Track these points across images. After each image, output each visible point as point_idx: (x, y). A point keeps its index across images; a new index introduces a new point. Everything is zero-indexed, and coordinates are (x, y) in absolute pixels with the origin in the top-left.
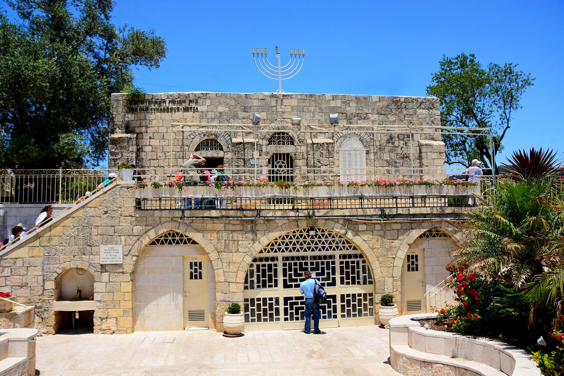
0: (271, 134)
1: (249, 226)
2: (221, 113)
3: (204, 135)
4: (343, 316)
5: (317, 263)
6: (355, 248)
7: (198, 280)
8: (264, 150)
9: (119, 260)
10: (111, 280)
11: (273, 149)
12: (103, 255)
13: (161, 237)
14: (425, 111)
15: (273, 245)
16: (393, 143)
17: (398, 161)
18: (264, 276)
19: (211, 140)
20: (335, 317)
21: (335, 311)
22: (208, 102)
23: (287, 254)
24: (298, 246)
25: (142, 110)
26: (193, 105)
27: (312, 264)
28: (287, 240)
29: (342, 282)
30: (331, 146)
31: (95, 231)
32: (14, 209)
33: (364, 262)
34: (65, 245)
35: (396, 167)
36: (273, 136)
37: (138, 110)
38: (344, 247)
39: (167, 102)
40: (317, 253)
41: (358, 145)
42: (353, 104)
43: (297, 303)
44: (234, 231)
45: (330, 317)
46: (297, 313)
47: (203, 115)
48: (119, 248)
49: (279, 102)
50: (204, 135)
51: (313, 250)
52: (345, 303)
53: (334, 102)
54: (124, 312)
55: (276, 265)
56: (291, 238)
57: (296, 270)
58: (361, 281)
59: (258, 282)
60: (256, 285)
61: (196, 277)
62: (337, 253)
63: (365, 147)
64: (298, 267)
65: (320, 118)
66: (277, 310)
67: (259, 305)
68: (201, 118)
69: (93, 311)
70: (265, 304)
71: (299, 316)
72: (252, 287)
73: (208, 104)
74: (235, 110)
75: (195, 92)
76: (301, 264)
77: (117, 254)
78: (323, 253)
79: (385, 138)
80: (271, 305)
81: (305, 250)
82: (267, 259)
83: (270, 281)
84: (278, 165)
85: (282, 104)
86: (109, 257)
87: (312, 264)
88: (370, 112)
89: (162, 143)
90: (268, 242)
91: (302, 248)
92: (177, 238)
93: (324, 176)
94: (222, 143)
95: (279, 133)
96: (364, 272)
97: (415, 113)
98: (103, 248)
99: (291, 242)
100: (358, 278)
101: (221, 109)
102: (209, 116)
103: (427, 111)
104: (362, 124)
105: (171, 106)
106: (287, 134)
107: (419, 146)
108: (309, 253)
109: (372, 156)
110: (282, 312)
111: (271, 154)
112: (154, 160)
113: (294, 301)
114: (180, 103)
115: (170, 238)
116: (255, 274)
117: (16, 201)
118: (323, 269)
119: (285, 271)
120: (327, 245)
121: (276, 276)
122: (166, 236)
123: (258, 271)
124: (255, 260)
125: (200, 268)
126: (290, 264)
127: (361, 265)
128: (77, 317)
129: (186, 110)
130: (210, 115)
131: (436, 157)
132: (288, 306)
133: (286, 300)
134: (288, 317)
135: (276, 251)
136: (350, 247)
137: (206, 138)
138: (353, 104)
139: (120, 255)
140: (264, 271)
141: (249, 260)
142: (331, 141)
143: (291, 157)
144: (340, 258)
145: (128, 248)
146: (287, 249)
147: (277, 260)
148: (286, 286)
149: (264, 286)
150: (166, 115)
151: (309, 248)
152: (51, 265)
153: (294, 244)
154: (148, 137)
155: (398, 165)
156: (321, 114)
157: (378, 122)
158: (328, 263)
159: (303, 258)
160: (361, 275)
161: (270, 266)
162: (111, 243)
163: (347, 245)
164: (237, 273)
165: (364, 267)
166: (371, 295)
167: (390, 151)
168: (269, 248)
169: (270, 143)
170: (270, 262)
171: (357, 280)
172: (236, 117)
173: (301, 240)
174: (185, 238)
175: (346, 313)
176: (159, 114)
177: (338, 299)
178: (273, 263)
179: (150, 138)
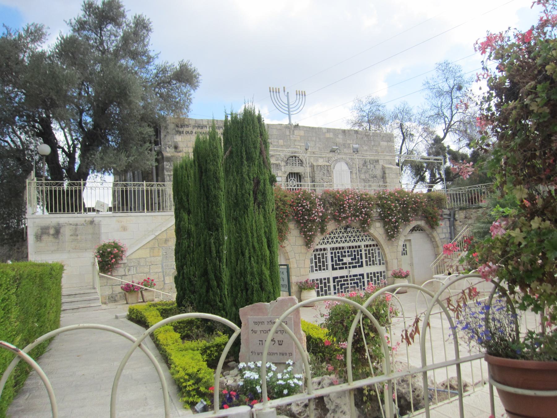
0: (287, 157)
5: (351, 251)
6: (373, 240)
11: (290, 169)
16: (367, 167)
17: (370, 179)
23: (333, 245)
25: (187, 132)
27: (348, 252)
28: (332, 236)
30: (329, 167)
33: (379, 249)
40: (351, 244)
41: (345, 167)
42: (340, 136)
46: (341, 288)
53: (328, 134)
55: (326, 254)
56: (335, 234)
58: (378, 262)
59: (316, 267)
62: (362, 244)
63: (349, 169)
66: (329, 287)
70: (321, 283)
71: (343, 290)
76: (341, 252)
78: (354, 244)
79: (362, 162)
80: (325, 283)
82: (321, 250)
83: (324, 266)
85: (293, 134)
87: (348, 252)
91: (341, 241)
95: (292, 157)
96: (379, 257)
97: (379, 144)
99: (335, 237)
108: (346, 245)
109: (354, 176)
111: (288, 173)
117: (119, 210)
119: (332, 257)
123: (315, 259)
127: (377, 251)
133: (334, 278)
134: (336, 291)
135: (326, 244)
136: (370, 239)
140: (319, 258)
142: (328, 164)
143: (300, 176)
148: (334, 269)
158: (358, 251)
159: (343, 248)
160: (378, 258)
161: (323, 254)
163: (368, 238)
165: (379, 253)
166: (384, 272)
167: (365, 172)
170: (322, 252)
173: (341, 235)
178: (325, 252)
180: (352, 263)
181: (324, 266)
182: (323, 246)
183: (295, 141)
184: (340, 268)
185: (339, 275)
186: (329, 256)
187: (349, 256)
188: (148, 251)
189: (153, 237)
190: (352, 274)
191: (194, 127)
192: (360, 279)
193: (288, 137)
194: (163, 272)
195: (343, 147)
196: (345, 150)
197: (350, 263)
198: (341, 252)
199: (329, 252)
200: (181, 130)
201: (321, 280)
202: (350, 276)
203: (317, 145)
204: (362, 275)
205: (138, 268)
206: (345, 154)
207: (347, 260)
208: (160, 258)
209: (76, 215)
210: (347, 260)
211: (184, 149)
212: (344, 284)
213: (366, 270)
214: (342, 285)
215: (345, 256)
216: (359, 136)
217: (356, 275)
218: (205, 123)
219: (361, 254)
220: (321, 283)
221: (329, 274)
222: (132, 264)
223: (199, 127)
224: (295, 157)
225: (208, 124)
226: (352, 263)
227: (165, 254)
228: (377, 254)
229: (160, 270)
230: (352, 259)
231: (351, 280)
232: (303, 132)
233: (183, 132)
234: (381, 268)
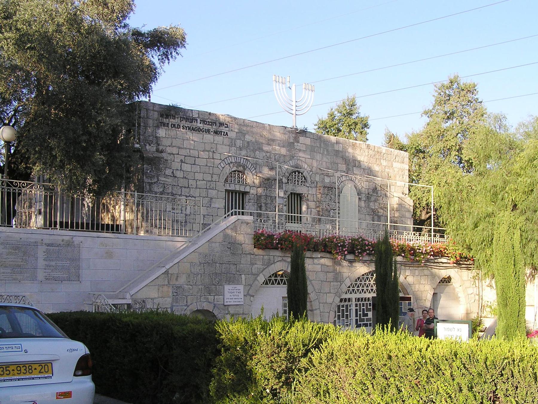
0: (290, 173)
2: (248, 142)
9: (241, 300)
12: (227, 295)
19: (238, 171)
23: (358, 296)
26: (223, 129)
32: (89, 239)
34: (192, 284)
44: (328, 272)
48: (241, 287)
77: (239, 294)
86: (232, 297)
98: (227, 288)
111: (289, 193)
112: (185, 187)
119: (356, 310)
124: (341, 300)
129: (216, 132)
130: (239, 143)
135: (351, 293)
137: (235, 169)
139: (241, 296)
152: (179, 307)
154: (179, 160)
161: (347, 306)
179: (181, 161)
182: (348, 296)
186: (354, 308)
189: (163, 270)
199: (354, 302)
200: (165, 121)
211: (168, 148)
216: (371, 152)
218: (196, 116)
224: (299, 172)
225: (199, 117)
233: (168, 124)
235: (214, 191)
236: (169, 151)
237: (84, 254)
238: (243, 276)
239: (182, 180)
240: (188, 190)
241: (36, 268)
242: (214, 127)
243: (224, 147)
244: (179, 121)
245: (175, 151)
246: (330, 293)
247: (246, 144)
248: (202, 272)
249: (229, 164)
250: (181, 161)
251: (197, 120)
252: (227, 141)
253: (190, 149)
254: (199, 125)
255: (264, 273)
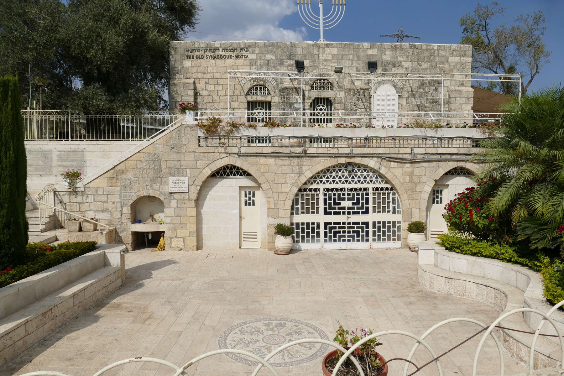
0: (313, 81)
1: (296, 162)
2: (268, 61)
3: (254, 81)
4: (374, 240)
5: (353, 195)
6: (386, 182)
7: (252, 207)
8: (307, 95)
10: (179, 206)
11: (315, 94)
12: (171, 184)
13: (221, 170)
14: (457, 59)
15: (315, 178)
17: (427, 105)
18: (307, 204)
20: (367, 240)
21: (367, 235)
22: (257, 50)
23: (327, 186)
24: (337, 179)
25: (198, 57)
26: (244, 53)
28: (328, 175)
29: (374, 211)
31: (163, 165)
33: (394, 194)
35: (426, 111)
36: (315, 81)
37: (195, 57)
38: (377, 181)
39: (221, 50)
40: (353, 186)
41: (392, 90)
43: (335, 228)
44: (283, 165)
45: (363, 240)
46: (335, 236)
47: (252, 63)
48: (186, 179)
49: (321, 50)
50: (254, 81)
51: (350, 183)
52: (377, 229)
54: (190, 232)
55: (317, 195)
57: (335, 199)
58: (391, 209)
59: (303, 209)
60: (300, 210)
61: (250, 204)
62: (371, 186)
63: (398, 92)
64: (337, 197)
65: (358, 66)
66: (318, 233)
67: (303, 229)
68: (251, 65)
69: (164, 232)
70: (308, 228)
71: (337, 239)
72: (297, 214)
73: (257, 52)
74: (282, 57)
75: (246, 41)
76: (339, 195)
78: (359, 186)
80: (313, 229)
81: (343, 183)
83: (313, 208)
84: (319, 108)
86: (177, 186)
87: (349, 195)
88: (404, 59)
89: (217, 87)
90: (311, 175)
92: (234, 171)
93: (361, 119)
94: (270, 88)
95: (320, 80)
96: (394, 203)
98: (171, 179)
100: (389, 208)
101: (269, 57)
102: (258, 64)
103: (459, 58)
104: (395, 71)
105: (223, 53)
106: (328, 80)
107: (448, 91)
108: (346, 186)
109: (404, 101)
110: (322, 234)
111: (313, 98)
113: (333, 226)
114: (233, 50)
115: (228, 171)
116: (300, 201)
118: (358, 199)
119: (325, 200)
120: (362, 179)
121: (317, 204)
122: (224, 169)
124: (300, 190)
125: (254, 196)
126: (330, 194)
127: (391, 196)
128: (150, 238)
129: (237, 57)
131: (464, 102)
132: (328, 230)
133: (326, 224)
137: (256, 83)
138: (388, 52)
139: (186, 185)
140: (307, 199)
141: (295, 190)
142: (367, 87)
143: (331, 101)
144: (373, 190)
145: (193, 179)
146: (327, 181)
147: (319, 191)
148: (326, 213)
149: (308, 212)
150: (219, 62)
151: (347, 181)
153: (334, 178)
155: (428, 109)
156: (358, 62)
157: (410, 70)
158: (362, 194)
159: (341, 189)
160: (391, 205)
162: (178, 175)
163: (379, 179)
164: (285, 201)
165: (394, 199)
168: (312, 180)
169: (312, 88)
171: (387, 210)
172: (282, 64)
174: (241, 171)
175: (377, 238)
176: (213, 61)
177: (371, 225)
178: (315, 193)
179: (206, 83)
180: (353, 208)
181: (313, 208)
183: (326, 60)
184: (335, 213)
185: (333, 221)
187: (349, 199)
188: (106, 180)
190: (351, 221)
191: (206, 50)
192: (362, 228)
193: (316, 56)
194: (121, 203)
195: (390, 66)
196: (393, 69)
197: (349, 208)
198: (339, 195)
201: (308, 224)
202: (349, 223)
203: (354, 65)
204: (367, 224)
205: (96, 197)
206: (394, 75)
207: (346, 204)
208: (118, 189)
209: (64, 142)
210: (346, 204)
212: (340, 232)
213: (371, 218)
214: (335, 233)
215: (344, 199)
216: (416, 51)
217: (358, 223)
219: (367, 200)
220: (308, 227)
221: (320, 218)
222: (90, 193)
223: (210, 50)
226: (353, 208)
227: (123, 184)
228: (391, 200)
229: (118, 200)
230: (353, 204)
231: (349, 228)
232: (336, 50)
233: (193, 56)
234: (397, 218)
235: (236, 103)
236: (195, 77)
237: (88, 156)
238: (188, 170)
239: (207, 97)
240: (212, 104)
241: (51, 167)
242: (235, 52)
243: (245, 67)
244: (203, 53)
245: (200, 75)
246: (285, 183)
247: (266, 62)
248: (147, 167)
249: (250, 80)
250: (206, 83)
251: (219, 49)
252: (247, 62)
253: (213, 73)
254: (221, 53)
255: (209, 166)
